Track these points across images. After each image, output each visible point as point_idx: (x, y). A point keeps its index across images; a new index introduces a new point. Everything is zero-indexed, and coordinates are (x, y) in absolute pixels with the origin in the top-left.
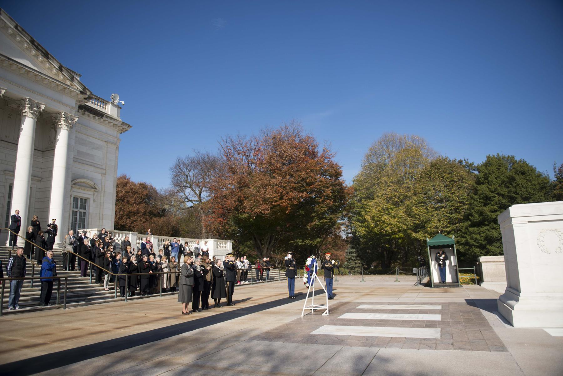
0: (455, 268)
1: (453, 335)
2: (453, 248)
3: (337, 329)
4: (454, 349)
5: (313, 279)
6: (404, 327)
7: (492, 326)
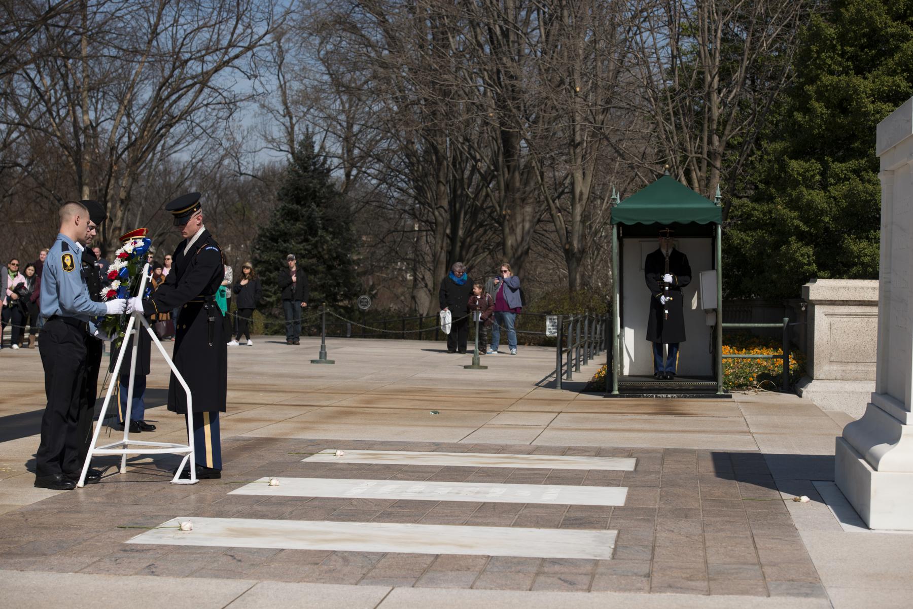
0: (711, 322)
1: (657, 550)
2: (714, 238)
3: (232, 530)
4: (651, 590)
5: (132, 336)
6: (487, 524)
7: (797, 526)
